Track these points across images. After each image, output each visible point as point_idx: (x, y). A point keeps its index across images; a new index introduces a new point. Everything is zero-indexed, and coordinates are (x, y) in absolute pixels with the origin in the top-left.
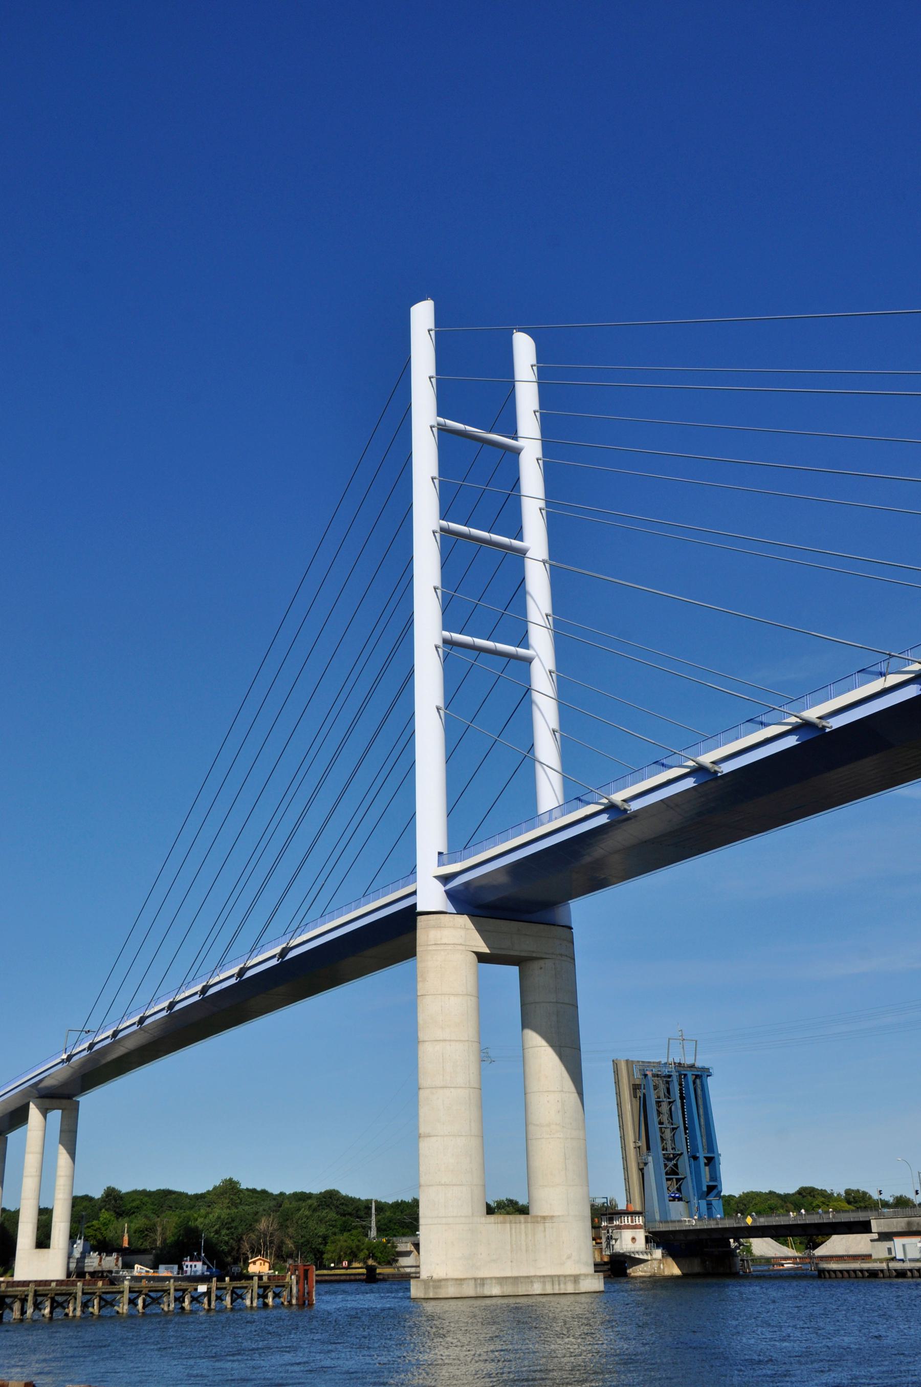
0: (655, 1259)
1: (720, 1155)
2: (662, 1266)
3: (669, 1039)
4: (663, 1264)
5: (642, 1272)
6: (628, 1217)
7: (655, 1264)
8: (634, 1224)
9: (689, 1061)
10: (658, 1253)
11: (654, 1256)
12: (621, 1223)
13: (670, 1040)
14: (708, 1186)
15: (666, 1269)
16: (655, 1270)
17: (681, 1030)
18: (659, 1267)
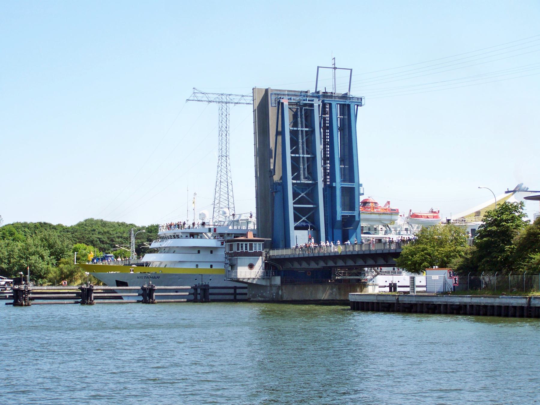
0: (275, 286)
1: (360, 185)
2: (280, 293)
3: (318, 67)
4: (282, 290)
5: (261, 297)
6: (260, 244)
7: (274, 290)
8: (254, 250)
9: (341, 90)
10: (277, 280)
11: (273, 283)
12: (238, 249)
13: (320, 68)
14: (343, 216)
15: (285, 295)
16: (273, 296)
17: (334, 58)
18: (277, 293)
